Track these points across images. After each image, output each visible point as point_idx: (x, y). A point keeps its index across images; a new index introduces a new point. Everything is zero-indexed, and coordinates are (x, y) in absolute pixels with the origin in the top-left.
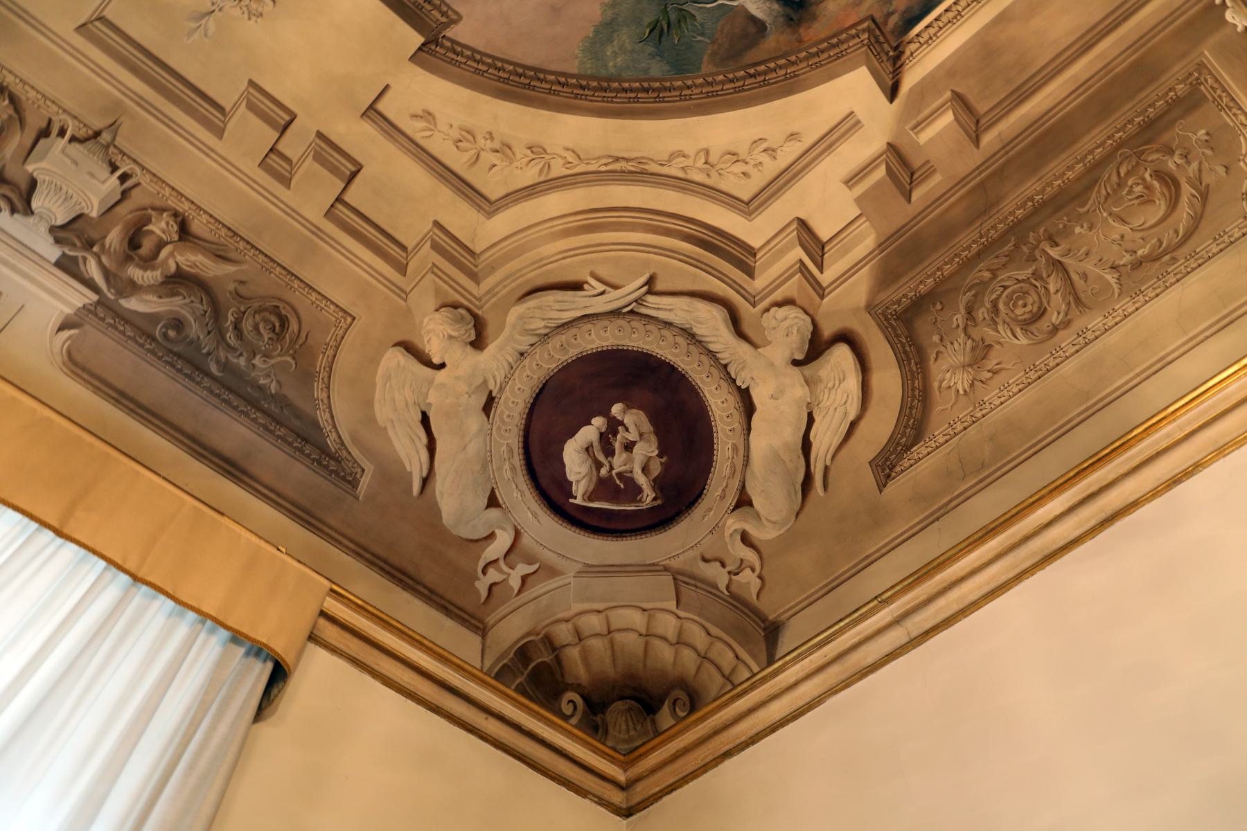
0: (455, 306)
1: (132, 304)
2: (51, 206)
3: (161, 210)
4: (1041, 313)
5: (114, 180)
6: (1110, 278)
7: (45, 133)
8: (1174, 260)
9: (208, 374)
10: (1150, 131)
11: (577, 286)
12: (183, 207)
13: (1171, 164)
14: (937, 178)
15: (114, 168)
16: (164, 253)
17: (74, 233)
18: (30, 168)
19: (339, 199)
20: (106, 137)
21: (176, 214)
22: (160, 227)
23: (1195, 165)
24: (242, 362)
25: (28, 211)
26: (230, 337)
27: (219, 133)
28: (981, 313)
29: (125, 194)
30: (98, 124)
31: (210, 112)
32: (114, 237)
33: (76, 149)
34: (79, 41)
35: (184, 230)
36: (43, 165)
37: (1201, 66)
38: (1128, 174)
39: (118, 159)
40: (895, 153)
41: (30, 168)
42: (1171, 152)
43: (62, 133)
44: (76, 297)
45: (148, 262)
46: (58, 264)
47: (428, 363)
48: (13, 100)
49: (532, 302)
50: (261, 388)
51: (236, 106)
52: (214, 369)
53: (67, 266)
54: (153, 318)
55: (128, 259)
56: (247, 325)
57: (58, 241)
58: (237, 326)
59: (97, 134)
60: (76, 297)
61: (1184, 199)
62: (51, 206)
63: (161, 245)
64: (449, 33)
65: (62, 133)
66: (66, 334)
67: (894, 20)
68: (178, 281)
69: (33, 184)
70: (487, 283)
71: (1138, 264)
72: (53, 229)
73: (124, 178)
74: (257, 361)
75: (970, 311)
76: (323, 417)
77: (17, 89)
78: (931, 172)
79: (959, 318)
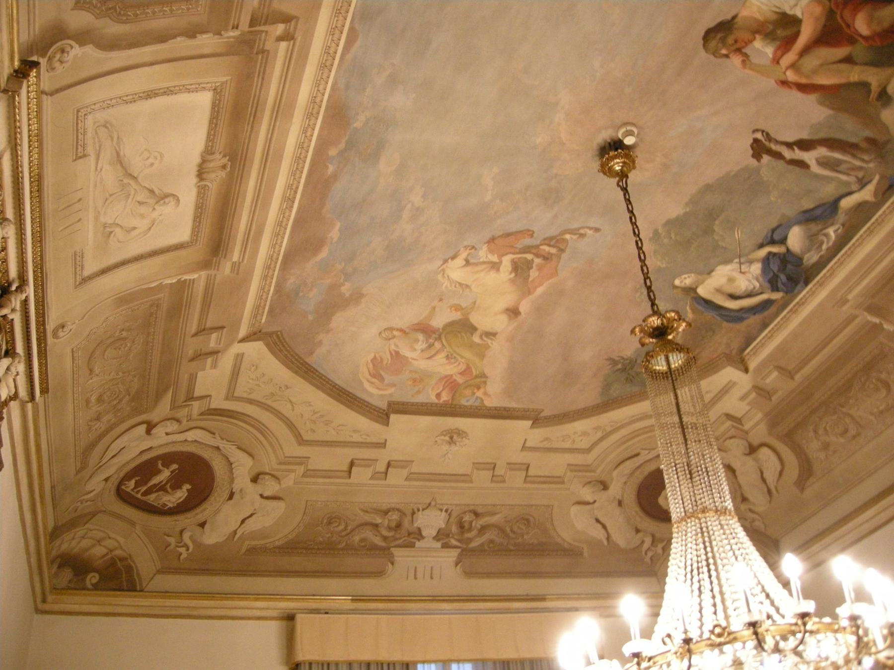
0: (590, 482)
1: (473, 545)
2: (429, 532)
3: (465, 513)
4: (846, 431)
5: (443, 513)
6: (871, 417)
7: (413, 513)
9: (511, 551)
11: (637, 455)
12: (471, 508)
13: (883, 376)
14: (780, 393)
15: (441, 510)
16: (473, 524)
17: (441, 535)
18: (415, 525)
19: (526, 476)
20: (433, 503)
21: (470, 511)
22: (467, 518)
24: (520, 540)
25: (423, 538)
26: (511, 535)
27: (471, 482)
28: (821, 432)
29: (450, 515)
30: (428, 501)
31: (465, 478)
32: (454, 529)
33: (426, 512)
34: (407, 483)
35: (477, 514)
36: (419, 522)
39: (441, 507)
40: (757, 388)
41: (415, 525)
42: (881, 372)
43: (419, 510)
44: (455, 553)
45: (470, 529)
46: (443, 547)
47: (588, 503)
48: (398, 510)
49: (621, 467)
50: (532, 544)
51: (472, 472)
52: (512, 548)
53: (446, 546)
54: (482, 544)
55: (463, 533)
56: (515, 528)
57: (438, 540)
58: (512, 531)
59: (430, 504)
60: (454, 554)
62: (429, 532)
63: (471, 523)
64: (542, 415)
65: (419, 510)
66: (459, 566)
67: (734, 352)
68: (483, 529)
69: (419, 529)
70: (599, 471)
71: (881, 412)
72: (434, 538)
73: (446, 511)
74: (525, 537)
75: (815, 431)
76: (559, 540)
77: (398, 506)
79: (811, 434)
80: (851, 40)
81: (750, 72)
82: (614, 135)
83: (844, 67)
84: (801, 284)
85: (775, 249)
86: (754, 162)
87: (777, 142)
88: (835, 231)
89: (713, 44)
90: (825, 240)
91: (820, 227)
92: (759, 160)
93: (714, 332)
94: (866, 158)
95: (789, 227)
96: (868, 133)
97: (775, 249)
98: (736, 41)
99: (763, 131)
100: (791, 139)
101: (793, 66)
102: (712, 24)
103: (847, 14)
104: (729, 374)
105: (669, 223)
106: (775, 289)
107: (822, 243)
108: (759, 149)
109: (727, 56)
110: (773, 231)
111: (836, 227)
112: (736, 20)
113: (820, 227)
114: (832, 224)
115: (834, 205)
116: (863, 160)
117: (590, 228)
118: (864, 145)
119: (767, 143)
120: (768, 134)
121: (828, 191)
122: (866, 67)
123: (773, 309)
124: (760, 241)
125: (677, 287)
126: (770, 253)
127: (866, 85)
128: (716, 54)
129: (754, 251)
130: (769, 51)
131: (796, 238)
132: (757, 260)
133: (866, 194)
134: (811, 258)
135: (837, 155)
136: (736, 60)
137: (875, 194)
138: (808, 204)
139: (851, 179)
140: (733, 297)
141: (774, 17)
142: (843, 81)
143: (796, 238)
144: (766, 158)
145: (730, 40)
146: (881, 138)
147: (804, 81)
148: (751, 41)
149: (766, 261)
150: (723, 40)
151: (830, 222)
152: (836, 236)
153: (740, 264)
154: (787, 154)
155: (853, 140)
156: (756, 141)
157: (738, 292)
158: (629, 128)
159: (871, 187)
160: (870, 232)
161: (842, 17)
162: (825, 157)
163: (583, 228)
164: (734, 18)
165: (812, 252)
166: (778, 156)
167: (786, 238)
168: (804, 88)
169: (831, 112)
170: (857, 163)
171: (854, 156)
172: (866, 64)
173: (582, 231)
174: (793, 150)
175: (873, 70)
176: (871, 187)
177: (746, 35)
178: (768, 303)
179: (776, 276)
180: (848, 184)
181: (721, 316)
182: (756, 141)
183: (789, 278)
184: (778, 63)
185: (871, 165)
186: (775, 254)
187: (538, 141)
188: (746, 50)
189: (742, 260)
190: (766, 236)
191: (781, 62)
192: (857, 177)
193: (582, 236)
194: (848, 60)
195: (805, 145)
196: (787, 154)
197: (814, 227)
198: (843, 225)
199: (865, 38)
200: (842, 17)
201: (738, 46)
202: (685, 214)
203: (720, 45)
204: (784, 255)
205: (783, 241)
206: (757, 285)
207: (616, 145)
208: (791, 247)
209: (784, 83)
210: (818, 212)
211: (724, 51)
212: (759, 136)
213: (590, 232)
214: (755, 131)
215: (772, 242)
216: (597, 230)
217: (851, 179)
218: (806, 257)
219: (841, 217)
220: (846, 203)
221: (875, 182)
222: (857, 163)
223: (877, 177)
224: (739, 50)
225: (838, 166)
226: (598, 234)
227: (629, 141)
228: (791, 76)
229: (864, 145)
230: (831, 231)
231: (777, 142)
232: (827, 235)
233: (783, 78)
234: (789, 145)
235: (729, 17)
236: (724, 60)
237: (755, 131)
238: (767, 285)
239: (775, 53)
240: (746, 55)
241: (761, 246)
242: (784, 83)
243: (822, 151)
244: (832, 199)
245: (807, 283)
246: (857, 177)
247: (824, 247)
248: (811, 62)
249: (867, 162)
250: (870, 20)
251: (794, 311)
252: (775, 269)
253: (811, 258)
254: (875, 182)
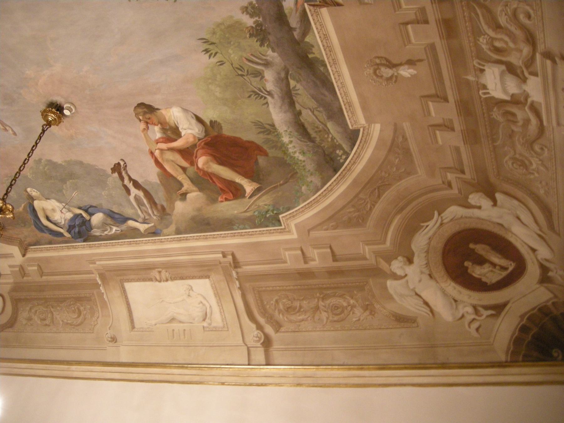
4: (44, 319)
6: (61, 323)
8: (74, 328)
10: (79, 299)
13: (82, 308)
14: (30, 278)
23: (85, 312)
28: (33, 311)
37: (93, 294)
38: (72, 304)
40: (22, 268)
61: (81, 317)
67: (26, 242)
71: (67, 324)
75: (31, 309)
78: (29, 276)
79: (28, 308)
80: (192, 163)
81: (143, 136)
82: (63, 103)
83: (180, 170)
84: (82, 239)
85: (84, 215)
86: (110, 171)
87: (127, 173)
88: (116, 230)
89: (140, 110)
90: (109, 230)
91: (112, 223)
92: (112, 173)
93: (25, 226)
94: (155, 213)
95: (99, 211)
96: (165, 204)
97: (84, 215)
98: (149, 119)
99: (125, 163)
100: (133, 177)
101: (162, 150)
102: (147, 103)
103: (200, 152)
104: (15, 250)
105: (50, 162)
106: (69, 231)
107: (106, 230)
108: (117, 168)
109: (140, 120)
110: (91, 206)
111: (118, 229)
112: (157, 111)
113: (112, 223)
114: (118, 227)
115: (126, 219)
116: (153, 212)
117: (13, 130)
118: (159, 207)
119: (122, 169)
120: (126, 166)
121: (128, 212)
122: (188, 180)
123: (60, 239)
124: (82, 206)
125: (27, 192)
126: (81, 214)
127: (181, 185)
128: (137, 115)
129: (75, 207)
130: (158, 135)
131: (97, 218)
132: (73, 213)
133: (142, 227)
134: (96, 232)
135: (145, 201)
136: (142, 126)
137: (146, 230)
138: (115, 209)
139: (142, 216)
140: (48, 218)
141: (173, 125)
142: (175, 175)
143: (97, 218)
144: (116, 175)
145: (148, 116)
146: (168, 211)
147: (160, 160)
148: (155, 125)
149: (76, 216)
150: (145, 113)
151: (118, 225)
152: (115, 233)
153: (64, 207)
154: (126, 181)
155: (157, 201)
156: (119, 164)
157: (52, 218)
158: (72, 107)
159: (146, 226)
160: (130, 244)
161: (197, 151)
162: (139, 196)
163: (10, 127)
164: (158, 109)
165: (99, 230)
166: (122, 179)
167: (93, 214)
168: (157, 162)
169: (159, 182)
170: (150, 212)
171: (151, 208)
172: (189, 178)
173: (7, 128)
174: (130, 182)
175: (190, 183)
176: (146, 226)
177: (155, 121)
178: (61, 235)
179: (74, 227)
180: (139, 216)
181: (35, 222)
182: (119, 164)
183: (79, 232)
184: (157, 143)
185: (155, 218)
186: (83, 217)
187: (27, 72)
188: (150, 126)
189: (67, 206)
190: (86, 206)
191: (159, 144)
192: (145, 217)
193: (6, 130)
194: (184, 169)
195: (136, 185)
196: (126, 181)
197: (109, 221)
198: (122, 231)
199: (198, 168)
200: (197, 151)
201: (148, 121)
202: (61, 165)
203: (142, 114)
204: (86, 220)
205: (91, 215)
206: (63, 223)
207: (59, 108)
208: (92, 220)
209: (152, 153)
210: (117, 216)
211: (141, 117)
212: (122, 163)
213: (11, 132)
214: (122, 160)
215: (86, 211)
216: (15, 134)
217: (142, 216)
218: (95, 230)
219: (124, 227)
220: (131, 223)
221: (150, 225)
222: (150, 212)
223: (153, 224)
224: (147, 123)
225: (142, 206)
226: (14, 136)
227: (66, 112)
228: (157, 153)
229: (159, 207)
230: (115, 228)
231: (127, 173)
232: (111, 229)
233: (153, 151)
234: (130, 179)
235: (156, 107)
236: (138, 121)
237: (122, 160)
238: (67, 226)
239: (160, 138)
240: (148, 128)
241: (80, 208)
242: (152, 153)
243: (141, 194)
244: (127, 216)
245: (84, 241)
246: (145, 217)
247: (106, 233)
248: (170, 156)
249: (154, 215)
250: (206, 163)
251: (68, 248)
252: (77, 223)
253: (96, 232)
254: (150, 225)
